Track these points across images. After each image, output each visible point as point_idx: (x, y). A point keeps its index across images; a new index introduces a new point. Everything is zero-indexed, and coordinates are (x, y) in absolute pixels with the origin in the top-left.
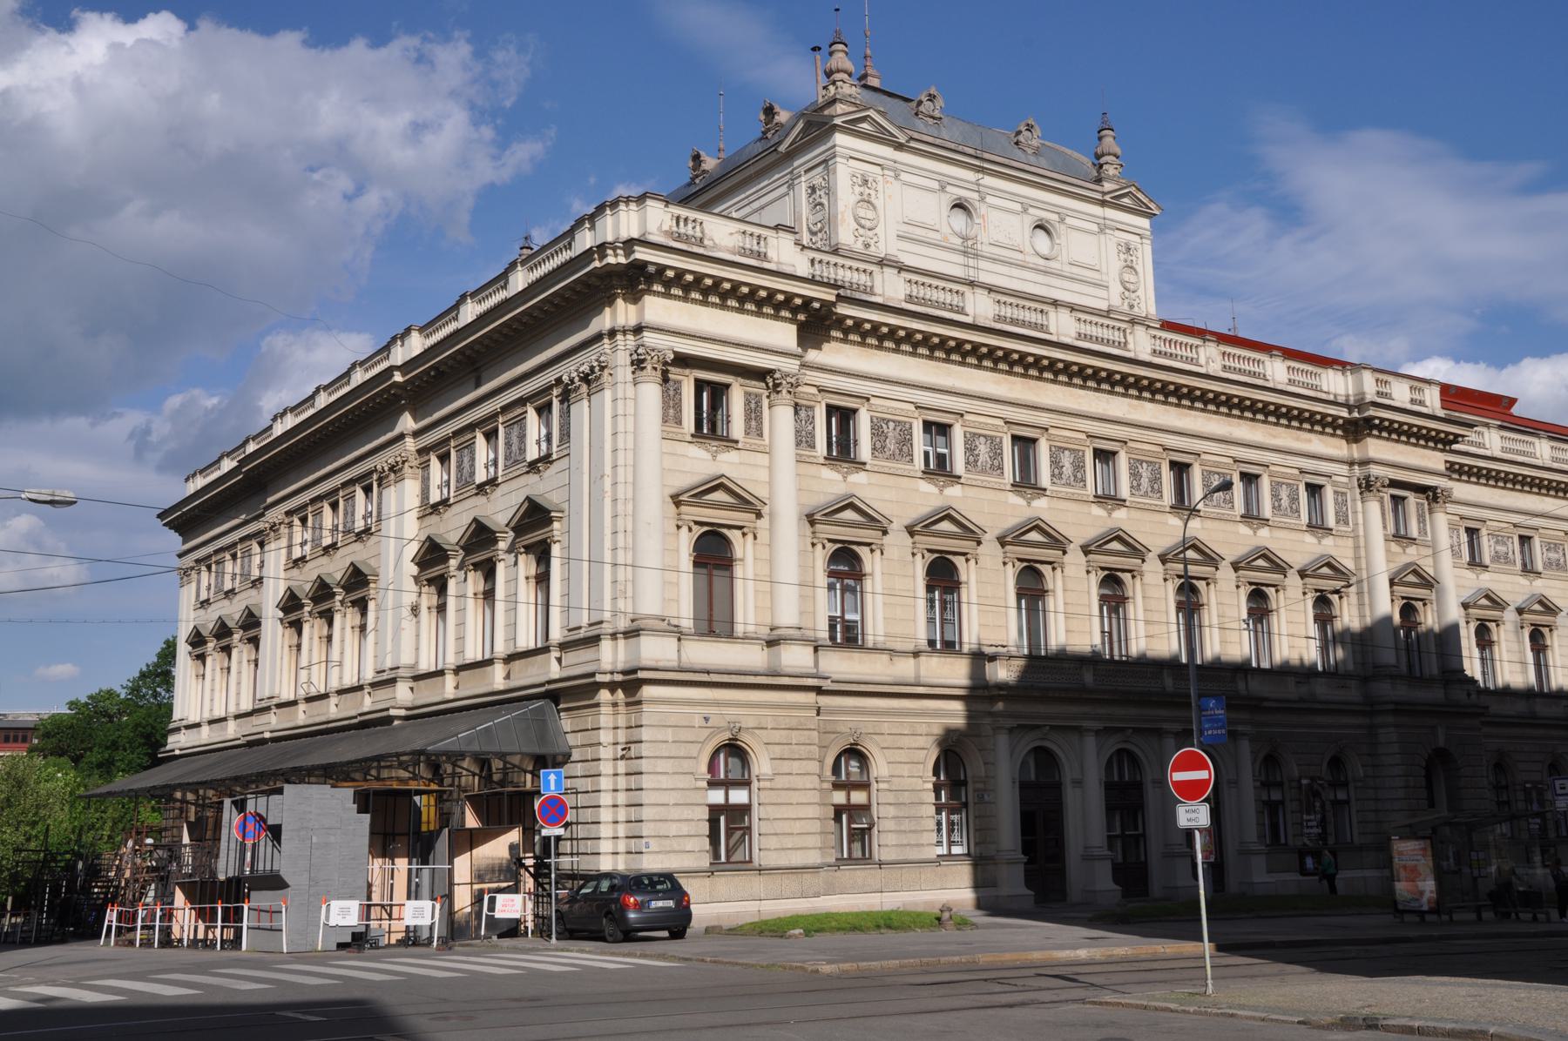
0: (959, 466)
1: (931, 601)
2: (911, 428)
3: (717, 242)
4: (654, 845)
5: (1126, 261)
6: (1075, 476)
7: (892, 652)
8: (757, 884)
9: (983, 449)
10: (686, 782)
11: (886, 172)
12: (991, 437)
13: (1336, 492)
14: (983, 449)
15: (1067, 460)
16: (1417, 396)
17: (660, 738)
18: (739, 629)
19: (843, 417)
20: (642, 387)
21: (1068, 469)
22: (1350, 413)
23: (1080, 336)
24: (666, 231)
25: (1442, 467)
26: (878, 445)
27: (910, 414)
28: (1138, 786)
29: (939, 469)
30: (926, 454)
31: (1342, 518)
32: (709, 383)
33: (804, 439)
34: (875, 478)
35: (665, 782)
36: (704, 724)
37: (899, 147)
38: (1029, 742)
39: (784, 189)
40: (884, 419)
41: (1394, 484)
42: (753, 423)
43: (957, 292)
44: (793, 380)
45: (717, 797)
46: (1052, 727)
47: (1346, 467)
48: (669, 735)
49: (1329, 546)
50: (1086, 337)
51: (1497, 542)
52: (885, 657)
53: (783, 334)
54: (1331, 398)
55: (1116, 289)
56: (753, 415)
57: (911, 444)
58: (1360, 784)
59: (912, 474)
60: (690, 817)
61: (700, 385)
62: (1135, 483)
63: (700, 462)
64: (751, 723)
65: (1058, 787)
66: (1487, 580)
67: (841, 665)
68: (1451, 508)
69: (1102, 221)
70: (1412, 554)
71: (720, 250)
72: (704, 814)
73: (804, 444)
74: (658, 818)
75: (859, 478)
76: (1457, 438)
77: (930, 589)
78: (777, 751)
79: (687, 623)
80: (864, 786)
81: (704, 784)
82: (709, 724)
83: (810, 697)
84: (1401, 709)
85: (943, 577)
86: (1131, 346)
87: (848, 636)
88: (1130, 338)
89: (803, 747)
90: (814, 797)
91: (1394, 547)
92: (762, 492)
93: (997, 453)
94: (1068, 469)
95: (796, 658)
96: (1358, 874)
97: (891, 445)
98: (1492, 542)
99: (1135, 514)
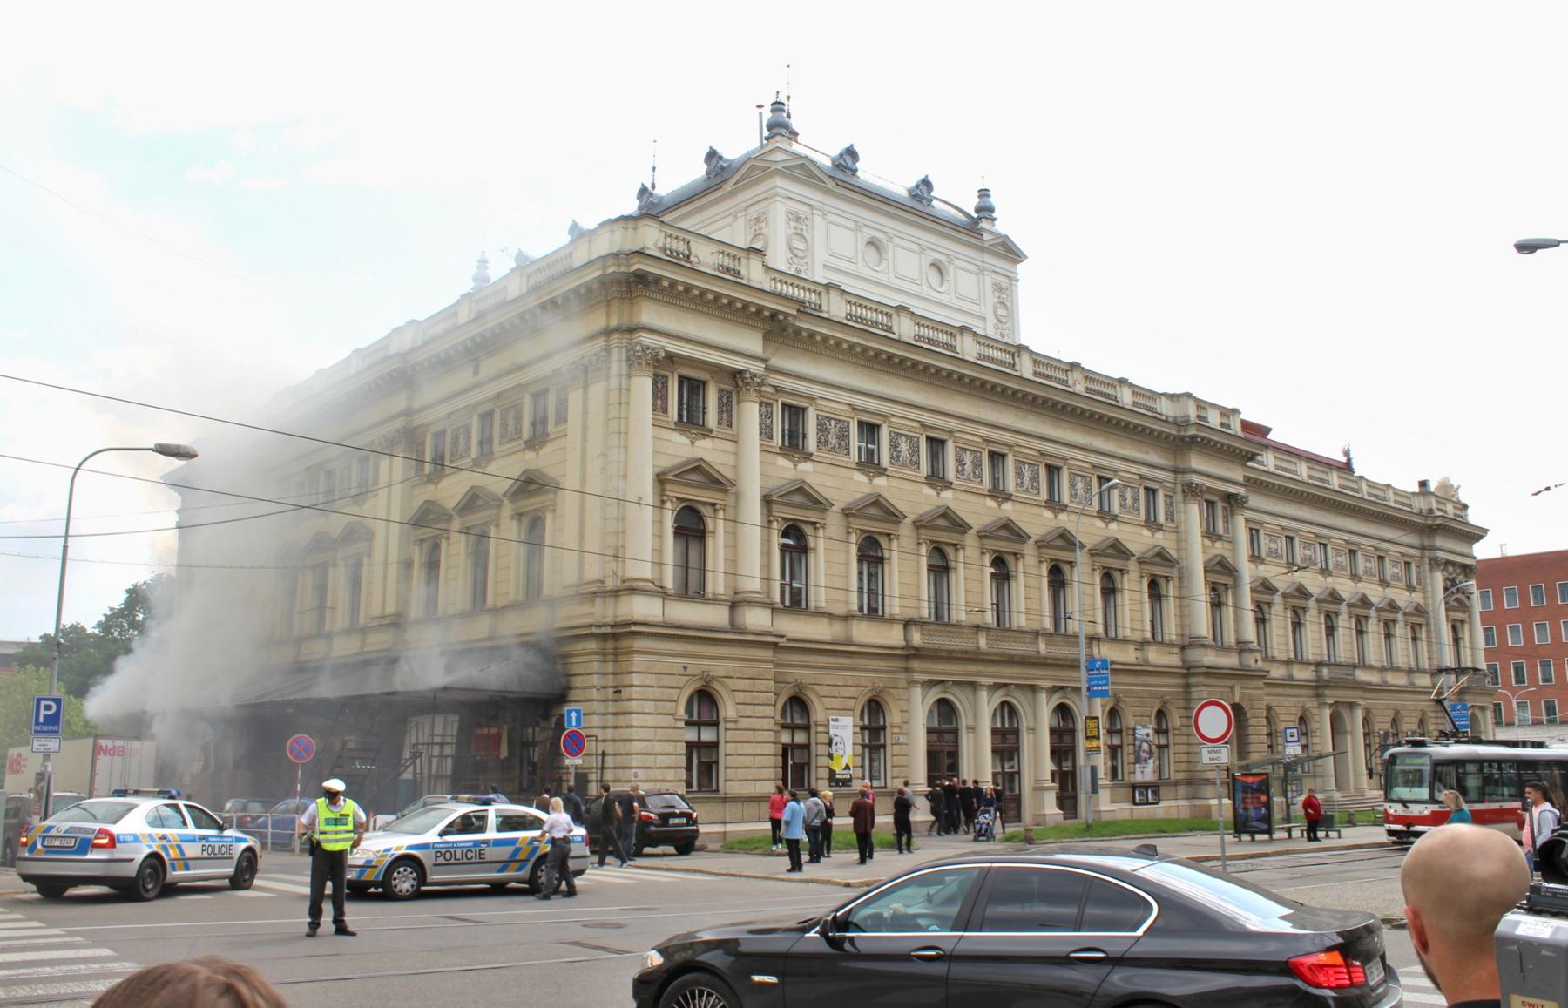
0: (885, 461)
1: (860, 573)
2: (848, 426)
5: (999, 297)
6: (974, 473)
7: (831, 617)
8: (730, 810)
9: (904, 446)
10: (668, 721)
11: (815, 211)
12: (911, 437)
13: (1166, 496)
14: (904, 446)
15: (968, 458)
16: (1225, 421)
17: (648, 683)
19: (795, 413)
21: (969, 467)
22: (1179, 431)
23: (980, 356)
24: (660, 248)
25: (1240, 479)
26: (822, 439)
27: (848, 414)
28: (1016, 732)
29: (870, 464)
30: (860, 448)
31: (1170, 516)
32: (689, 379)
33: (766, 432)
34: (819, 467)
35: (650, 720)
36: (682, 672)
37: (828, 192)
38: (934, 694)
39: (730, 219)
40: (827, 417)
41: (1210, 490)
42: (725, 415)
43: (887, 314)
44: (759, 380)
46: (955, 683)
47: (1172, 475)
48: (650, 680)
49: (1161, 539)
50: (986, 358)
51: (1271, 540)
52: (825, 621)
53: (752, 342)
54: (1164, 418)
55: (991, 321)
56: (725, 409)
58: (1177, 732)
59: (849, 465)
60: (671, 751)
61: (682, 379)
62: (1019, 481)
63: (681, 448)
64: (721, 673)
65: (955, 732)
66: (1264, 571)
67: (795, 627)
68: (1248, 514)
69: (979, 263)
70: (1219, 548)
71: (703, 265)
72: (682, 748)
74: (644, 751)
75: (806, 466)
76: (1252, 457)
77: (860, 560)
78: (741, 696)
79: (669, 583)
81: (682, 724)
83: (768, 654)
84: (1212, 672)
85: (871, 555)
86: (1017, 367)
87: (796, 602)
88: (1017, 360)
89: (761, 694)
90: (770, 736)
91: (1208, 543)
92: (729, 474)
93: (915, 450)
94: (969, 467)
95: (756, 619)
96: (1173, 803)
97: (833, 440)
98: (1267, 541)
99: (1019, 507)
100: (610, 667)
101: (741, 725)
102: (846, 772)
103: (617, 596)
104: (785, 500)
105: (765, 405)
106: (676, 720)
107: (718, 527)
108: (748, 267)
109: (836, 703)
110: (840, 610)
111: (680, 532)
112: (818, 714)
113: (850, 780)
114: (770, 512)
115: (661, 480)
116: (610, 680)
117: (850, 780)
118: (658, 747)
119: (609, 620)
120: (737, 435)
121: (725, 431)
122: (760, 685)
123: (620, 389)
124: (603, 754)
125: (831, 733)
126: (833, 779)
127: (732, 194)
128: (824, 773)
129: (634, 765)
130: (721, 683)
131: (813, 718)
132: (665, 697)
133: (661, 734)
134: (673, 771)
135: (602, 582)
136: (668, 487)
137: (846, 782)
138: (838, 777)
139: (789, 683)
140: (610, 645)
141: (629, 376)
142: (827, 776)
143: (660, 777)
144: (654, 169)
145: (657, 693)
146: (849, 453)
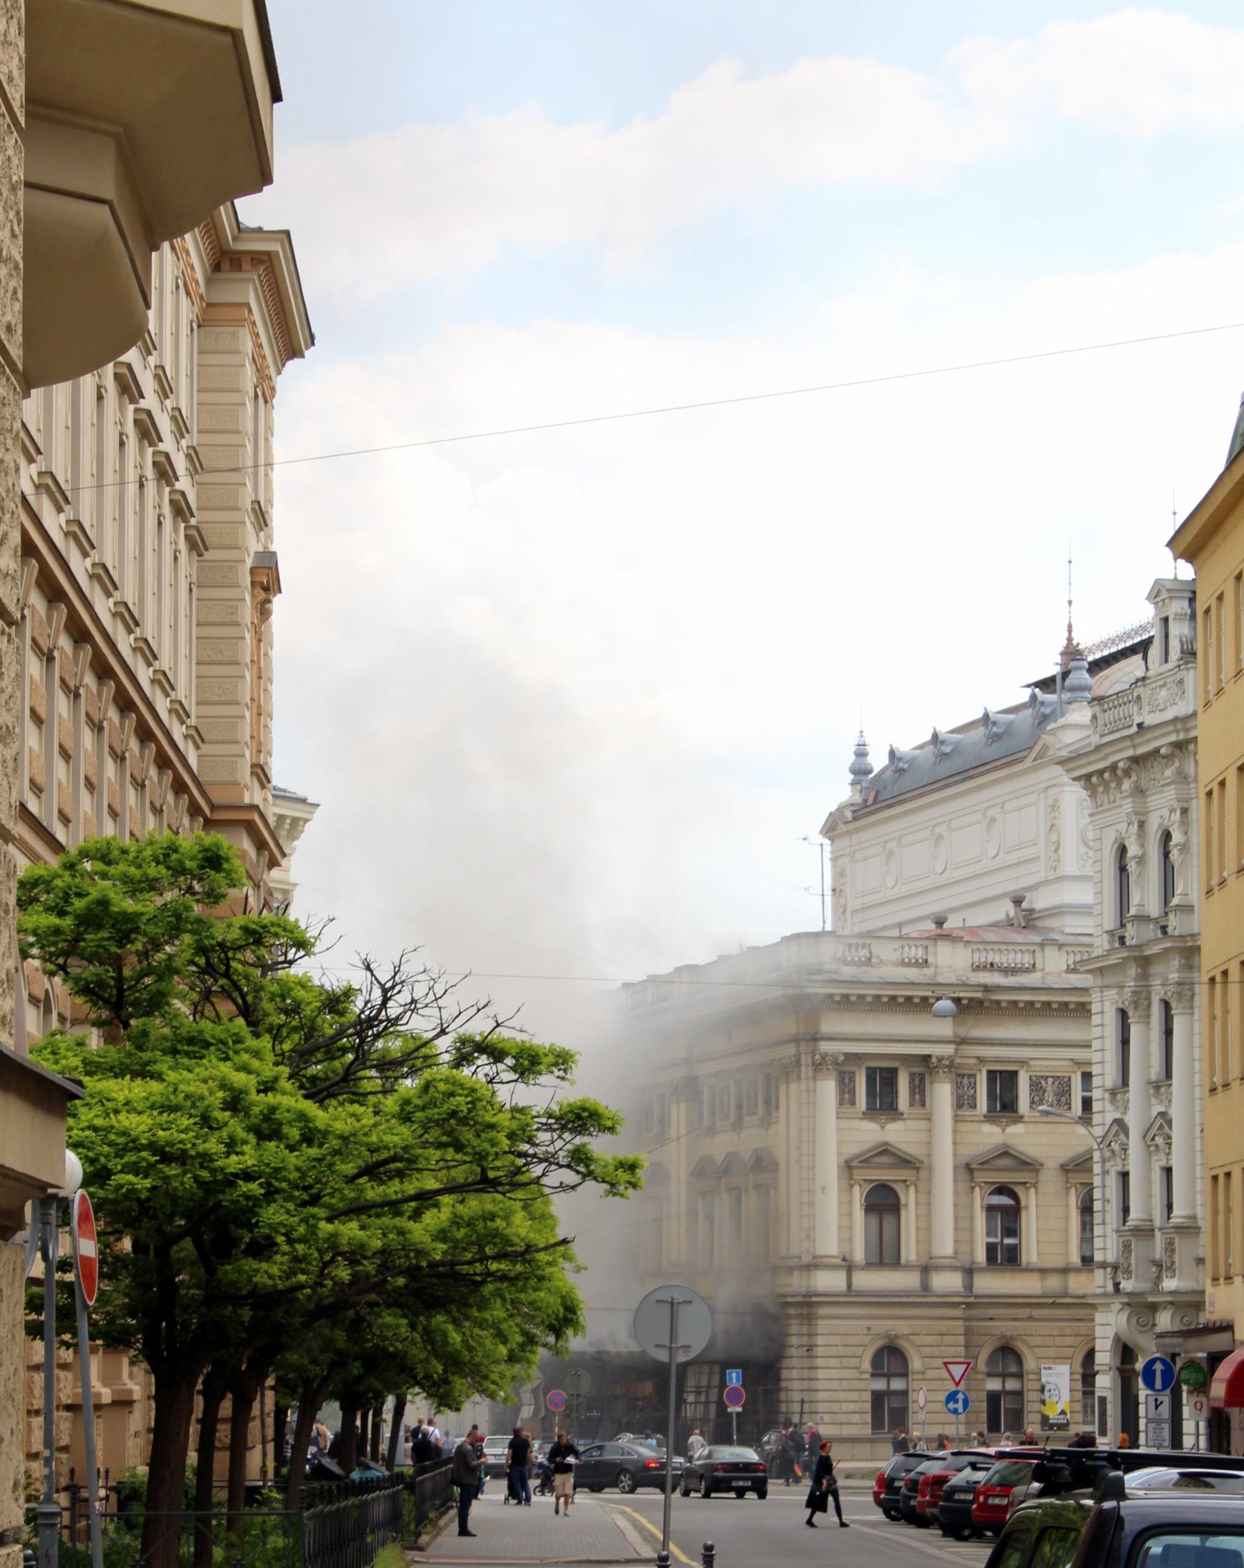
3: (883, 958)
4: (827, 1418)
7: (1043, 1271)
10: (853, 1374)
17: (831, 1342)
18: (903, 1261)
20: (820, 1084)
26: (1037, 1099)
33: (963, 1102)
34: (1032, 1127)
35: (834, 1374)
36: (866, 1332)
40: (1042, 1077)
42: (917, 1097)
45: (880, 1385)
57: (1070, 1095)
63: (869, 1133)
64: (906, 1331)
73: (966, 1106)
78: (928, 1351)
79: (859, 1256)
80: (1019, 1375)
81: (868, 1376)
82: (872, 1332)
100: (805, 1330)
101: (926, 1376)
102: (1062, 1416)
103: (809, 1270)
104: (986, 1166)
105: (962, 1079)
106: (861, 1373)
107: (909, 1199)
108: (936, 954)
109: (1052, 1352)
110: (1059, 1263)
111: (869, 1208)
112: (1030, 1364)
113: (1067, 1424)
114: (972, 1179)
115: (849, 1167)
116: (805, 1340)
117: (1067, 1424)
118: (843, 1396)
119: (803, 1290)
120: (930, 1113)
121: (918, 1111)
122: (947, 1339)
123: (808, 1091)
124: (802, 1402)
125: (1044, 1380)
126: (1045, 1419)
127: (1034, 769)
128: (1038, 1418)
129: (820, 1410)
130: (908, 1340)
131: (1025, 1367)
132: (849, 1354)
133: (845, 1385)
134: (858, 1415)
135: (800, 1258)
136: (855, 1171)
137: (1061, 1427)
138: (1051, 1421)
139: (994, 1335)
140: (805, 1311)
141: (815, 1079)
142: (1040, 1420)
143: (844, 1421)
144: (1070, 602)
145: (842, 1351)
146: (1070, 1108)
